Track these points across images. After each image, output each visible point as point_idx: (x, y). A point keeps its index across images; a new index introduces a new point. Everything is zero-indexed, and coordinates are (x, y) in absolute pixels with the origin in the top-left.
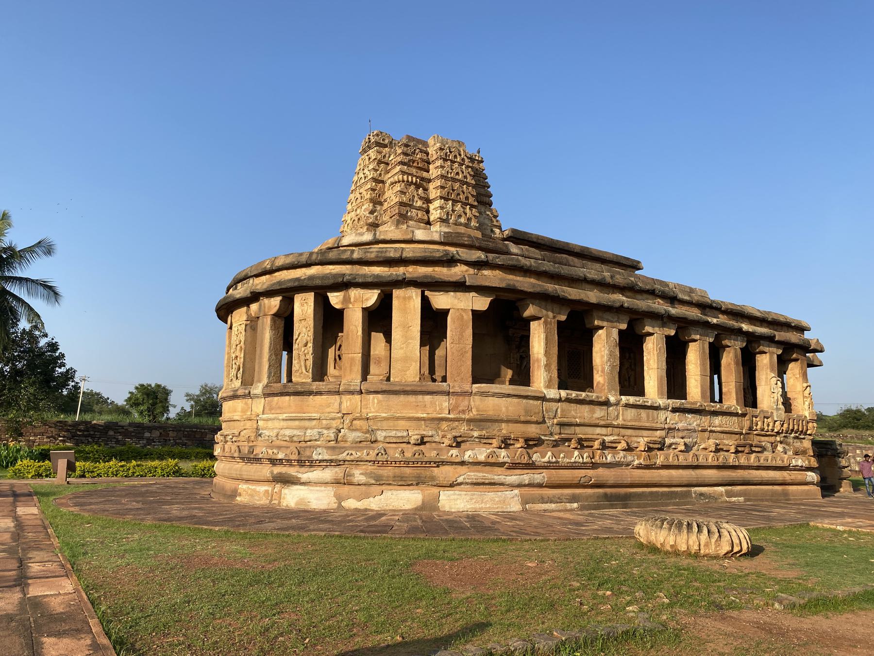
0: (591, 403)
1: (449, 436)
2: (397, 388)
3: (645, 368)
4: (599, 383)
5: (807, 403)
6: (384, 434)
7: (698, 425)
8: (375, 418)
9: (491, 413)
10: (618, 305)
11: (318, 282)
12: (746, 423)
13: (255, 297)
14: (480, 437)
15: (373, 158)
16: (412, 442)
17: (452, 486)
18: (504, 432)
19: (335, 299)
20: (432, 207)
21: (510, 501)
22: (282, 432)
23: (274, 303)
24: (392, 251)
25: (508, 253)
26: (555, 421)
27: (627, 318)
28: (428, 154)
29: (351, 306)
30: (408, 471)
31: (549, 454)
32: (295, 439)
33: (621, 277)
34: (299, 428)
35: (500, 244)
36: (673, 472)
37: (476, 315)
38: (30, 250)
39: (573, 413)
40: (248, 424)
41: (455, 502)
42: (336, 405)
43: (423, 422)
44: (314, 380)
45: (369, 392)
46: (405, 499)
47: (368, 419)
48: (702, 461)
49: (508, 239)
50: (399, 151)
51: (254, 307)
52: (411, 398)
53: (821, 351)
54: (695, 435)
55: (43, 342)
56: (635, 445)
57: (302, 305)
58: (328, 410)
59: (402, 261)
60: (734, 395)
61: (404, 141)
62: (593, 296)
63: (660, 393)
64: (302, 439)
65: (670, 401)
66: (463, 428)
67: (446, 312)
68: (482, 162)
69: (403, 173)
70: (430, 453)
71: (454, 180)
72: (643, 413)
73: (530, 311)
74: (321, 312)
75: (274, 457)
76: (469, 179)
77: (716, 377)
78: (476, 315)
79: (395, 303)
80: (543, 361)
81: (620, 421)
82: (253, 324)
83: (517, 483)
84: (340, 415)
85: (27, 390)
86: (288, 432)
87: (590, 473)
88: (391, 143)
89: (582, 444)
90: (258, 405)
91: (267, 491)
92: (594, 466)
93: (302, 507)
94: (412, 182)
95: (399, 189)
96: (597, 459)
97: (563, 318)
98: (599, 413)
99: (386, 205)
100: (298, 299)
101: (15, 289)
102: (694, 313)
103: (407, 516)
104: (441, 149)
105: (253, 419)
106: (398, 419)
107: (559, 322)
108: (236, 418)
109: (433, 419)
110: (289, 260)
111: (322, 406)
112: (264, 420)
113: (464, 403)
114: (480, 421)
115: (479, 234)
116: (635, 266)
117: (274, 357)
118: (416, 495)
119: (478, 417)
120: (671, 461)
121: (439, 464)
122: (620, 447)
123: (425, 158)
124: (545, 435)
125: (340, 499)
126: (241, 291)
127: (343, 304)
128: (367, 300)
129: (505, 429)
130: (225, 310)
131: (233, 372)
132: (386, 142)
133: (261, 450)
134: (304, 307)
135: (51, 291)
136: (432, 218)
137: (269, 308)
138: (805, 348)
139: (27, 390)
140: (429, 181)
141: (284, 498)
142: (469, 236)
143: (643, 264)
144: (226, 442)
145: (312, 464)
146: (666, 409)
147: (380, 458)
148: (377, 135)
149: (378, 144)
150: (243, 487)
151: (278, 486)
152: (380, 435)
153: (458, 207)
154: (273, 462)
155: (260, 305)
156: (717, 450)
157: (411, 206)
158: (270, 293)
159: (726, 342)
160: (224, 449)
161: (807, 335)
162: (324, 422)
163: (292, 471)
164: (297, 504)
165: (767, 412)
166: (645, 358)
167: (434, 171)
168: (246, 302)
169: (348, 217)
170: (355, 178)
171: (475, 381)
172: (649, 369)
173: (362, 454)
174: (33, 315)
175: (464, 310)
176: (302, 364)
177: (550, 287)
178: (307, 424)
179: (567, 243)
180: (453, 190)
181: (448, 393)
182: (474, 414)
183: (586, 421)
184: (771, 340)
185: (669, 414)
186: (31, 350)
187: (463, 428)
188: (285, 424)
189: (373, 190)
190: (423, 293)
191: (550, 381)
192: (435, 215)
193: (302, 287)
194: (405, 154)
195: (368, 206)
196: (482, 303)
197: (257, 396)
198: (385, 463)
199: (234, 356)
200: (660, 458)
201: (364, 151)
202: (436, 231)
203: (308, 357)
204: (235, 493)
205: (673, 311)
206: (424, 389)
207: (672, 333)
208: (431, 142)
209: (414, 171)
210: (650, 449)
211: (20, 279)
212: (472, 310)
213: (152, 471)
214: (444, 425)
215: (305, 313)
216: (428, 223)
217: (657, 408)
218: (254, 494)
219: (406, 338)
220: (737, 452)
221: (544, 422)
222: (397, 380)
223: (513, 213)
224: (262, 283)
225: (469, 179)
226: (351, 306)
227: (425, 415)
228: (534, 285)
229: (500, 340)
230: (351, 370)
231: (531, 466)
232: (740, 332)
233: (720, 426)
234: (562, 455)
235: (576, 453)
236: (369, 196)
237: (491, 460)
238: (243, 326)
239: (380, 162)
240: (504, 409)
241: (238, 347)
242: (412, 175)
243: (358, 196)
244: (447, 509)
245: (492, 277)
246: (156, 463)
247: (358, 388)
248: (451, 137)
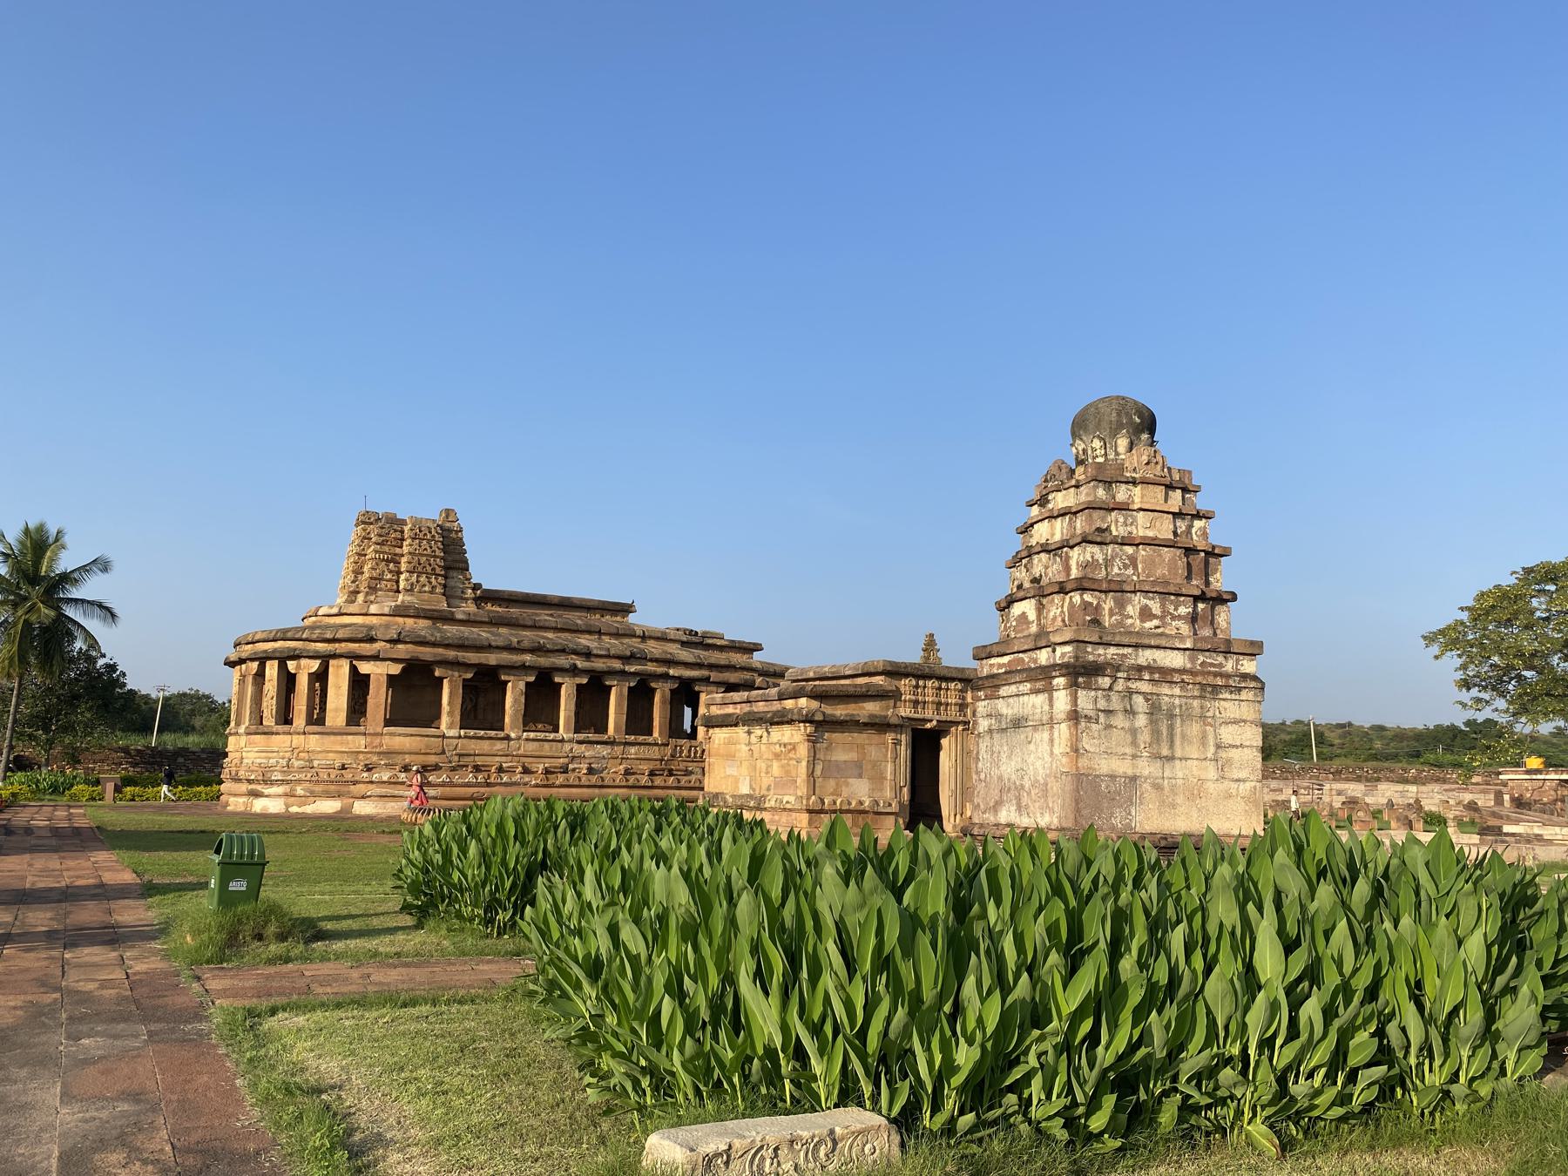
12: (669, 750)
13: (242, 661)
19: (291, 665)
20: (402, 577)
23: (255, 665)
28: (402, 532)
36: (574, 790)
37: (390, 677)
38: (85, 569)
41: (362, 808)
55: (101, 662)
62: (492, 659)
63: (567, 730)
66: (375, 758)
70: (348, 775)
72: (546, 745)
73: (437, 674)
76: (438, 553)
77: (688, 711)
85: (84, 714)
87: (483, 790)
89: (477, 769)
90: (243, 739)
92: (488, 785)
97: (469, 676)
98: (499, 745)
100: (268, 663)
101: (70, 612)
105: (245, 749)
110: (264, 636)
111: (281, 742)
113: (377, 741)
114: (388, 753)
116: (625, 609)
121: (355, 783)
125: (287, 806)
126: (233, 658)
130: (231, 664)
133: (242, 774)
134: (272, 669)
135: (109, 613)
139: (84, 714)
145: (272, 783)
146: (570, 741)
150: (232, 799)
152: (316, 763)
153: (423, 579)
154: (249, 781)
156: (627, 772)
159: (653, 685)
163: (259, 788)
167: (405, 549)
171: (388, 723)
173: (302, 776)
174: (88, 635)
177: (451, 654)
179: (545, 596)
185: (576, 746)
186: (88, 673)
187: (375, 758)
192: (402, 585)
195: (351, 577)
196: (396, 669)
200: (561, 779)
204: (227, 804)
205: (581, 663)
207: (585, 681)
209: (386, 549)
210: (547, 772)
211: (76, 601)
213: (197, 796)
214: (361, 757)
217: (562, 741)
218: (236, 804)
219: (338, 695)
220: (652, 774)
221: (443, 752)
223: (490, 569)
224: (247, 650)
225: (438, 553)
229: (413, 694)
232: (665, 676)
245: (403, 650)
246: (202, 788)
248: (431, 513)
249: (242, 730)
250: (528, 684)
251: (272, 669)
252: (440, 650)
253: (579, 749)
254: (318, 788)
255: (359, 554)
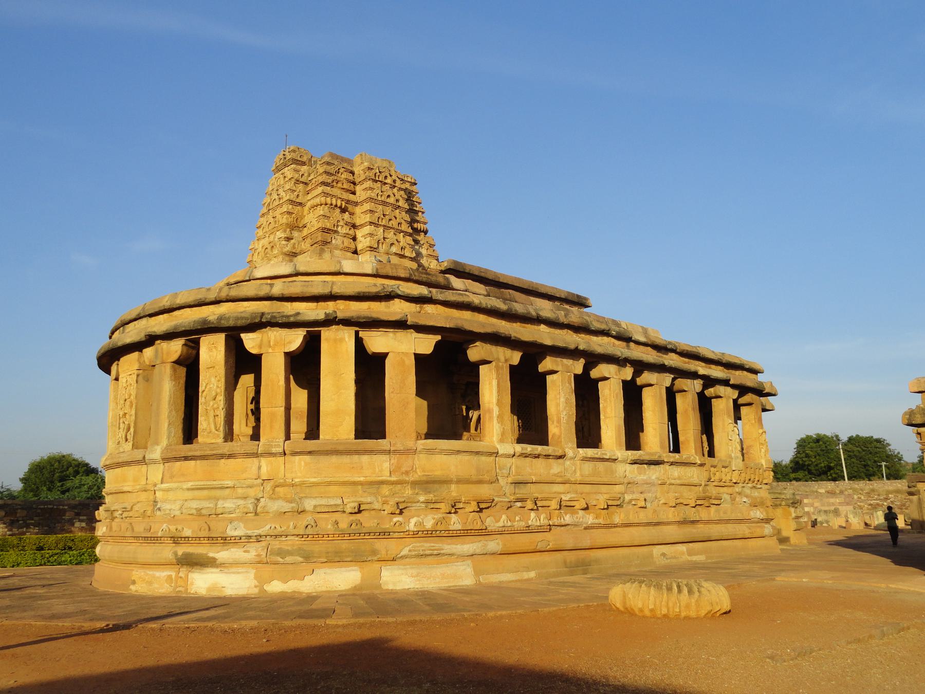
0: (547, 456)
1: (392, 502)
2: (328, 448)
3: (602, 417)
4: (554, 435)
5: (763, 450)
6: (314, 502)
7: (658, 478)
8: (302, 484)
9: (438, 473)
10: (572, 347)
11: (231, 323)
12: (705, 475)
13: (150, 340)
14: (427, 502)
15: (289, 177)
16: (348, 510)
17: (394, 560)
18: (454, 494)
19: (251, 341)
20: (359, 234)
21: (463, 575)
22: (187, 504)
23: (176, 347)
24: (318, 285)
25: (448, 287)
26: (510, 480)
27: (582, 361)
28: (353, 173)
29: (270, 350)
30: (344, 545)
31: (504, 517)
32: (204, 512)
33: (575, 315)
34: (209, 498)
35: (441, 279)
37: (419, 359)
39: (528, 470)
40: (143, 496)
41: (398, 579)
42: (254, 469)
43: (360, 487)
44: (226, 440)
45: (295, 454)
46: (341, 579)
47: (293, 485)
48: (663, 518)
49: (448, 271)
50: (321, 170)
51: (148, 352)
52: (346, 459)
53: (774, 395)
54: (654, 489)
56: (594, 503)
57: (210, 350)
58: (244, 476)
59: (331, 297)
60: (692, 445)
61: (327, 159)
64: (213, 512)
65: (630, 453)
67: (382, 357)
68: (415, 184)
69: (326, 194)
71: (384, 203)
72: (601, 466)
74: (232, 361)
75: (178, 535)
78: (419, 359)
79: (324, 346)
80: (496, 411)
81: (578, 477)
82: (146, 373)
83: (471, 552)
84: (259, 481)
86: (195, 505)
88: (310, 160)
90: (156, 473)
91: (170, 577)
93: (216, 594)
94: (336, 206)
95: (322, 212)
96: (555, 521)
98: (556, 468)
99: (305, 232)
102: (650, 356)
103: (343, 596)
104: (369, 169)
106: (329, 484)
107: (511, 367)
108: (126, 489)
109: (372, 483)
112: (163, 490)
114: (427, 484)
115: (414, 265)
117: (174, 412)
118: (353, 573)
119: (425, 478)
120: (633, 519)
122: (578, 505)
123: (351, 178)
124: (499, 496)
125: (261, 581)
127: (260, 347)
128: (290, 343)
129: (454, 491)
131: (122, 433)
132: (305, 159)
134: (212, 352)
136: (360, 247)
137: (168, 353)
138: (760, 392)
140: (356, 204)
141: (192, 584)
142: (405, 268)
143: (591, 302)
144: (113, 519)
145: (226, 541)
147: (309, 531)
148: (294, 151)
149: (295, 161)
151: (183, 571)
152: (309, 504)
154: (176, 540)
155: (157, 351)
157: (336, 232)
158: (169, 336)
160: (111, 528)
161: (760, 378)
162: (240, 491)
164: (209, 589)
165: (725, 461)
166: (601, 406)
167: (361, 193)
168: (138, 347)
169: (259, 245)
170: (267, 200)
172: (606, 418)
175: (406, 354)
176: (211, 419)
178: (218, 493)
180: (384, 215)
181: (389, 452)
182: (418, 475)
183: (543, 479)
184: (725, 383)
185: (629, 467)
187: (408, 492)
188: (190, 494)
189: (289, 213)
190: (357, 333)
191: (503, 434)
192: (363, 243)
193: (208, 329)
194: (327, 173)
197: (154, 462)
198: (317, 536)
199: (121, 413)
201: (278, 169)
202: (367, 263)
203: (218, 413)
206: (360, 448)
208: (357, 159)
209: (336, 191)
212: (415, 354)
214: (385, 490)
215: (209, 362)
216: (355, 252)
222: (327, 437)
225: (401, 203)
226: (270, 350)
227: (362, 479)
228: (483, 325)
230: (271, 427)
231: (484, 533)
233: (679, 478)
234: (517, 518)
235: (533, 514)
236: (284, 221)
237: (439, 527)
238: (134, 377)
239: (298, 182)
240: (453, 468)
241: (128, 403)
242: (337, 198)
243: (272, 220)
244: (391, 587)
245: (435, 315)
247: (281, 450)
249: (156, 453)
250: (576, 376)
251: (212, 352)
252: (482, 318)
253: (632, 472)
254: (317, 547)
255: (292, 202)
